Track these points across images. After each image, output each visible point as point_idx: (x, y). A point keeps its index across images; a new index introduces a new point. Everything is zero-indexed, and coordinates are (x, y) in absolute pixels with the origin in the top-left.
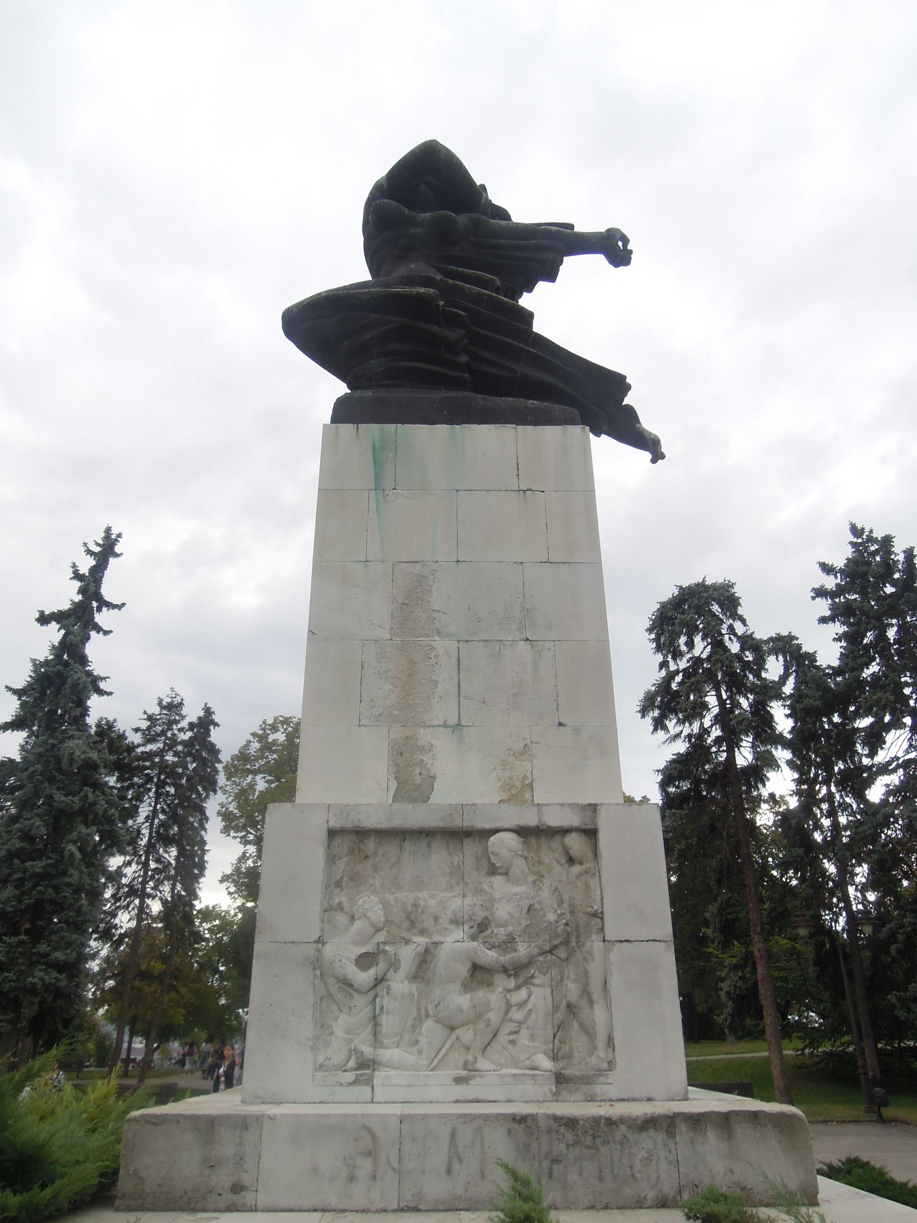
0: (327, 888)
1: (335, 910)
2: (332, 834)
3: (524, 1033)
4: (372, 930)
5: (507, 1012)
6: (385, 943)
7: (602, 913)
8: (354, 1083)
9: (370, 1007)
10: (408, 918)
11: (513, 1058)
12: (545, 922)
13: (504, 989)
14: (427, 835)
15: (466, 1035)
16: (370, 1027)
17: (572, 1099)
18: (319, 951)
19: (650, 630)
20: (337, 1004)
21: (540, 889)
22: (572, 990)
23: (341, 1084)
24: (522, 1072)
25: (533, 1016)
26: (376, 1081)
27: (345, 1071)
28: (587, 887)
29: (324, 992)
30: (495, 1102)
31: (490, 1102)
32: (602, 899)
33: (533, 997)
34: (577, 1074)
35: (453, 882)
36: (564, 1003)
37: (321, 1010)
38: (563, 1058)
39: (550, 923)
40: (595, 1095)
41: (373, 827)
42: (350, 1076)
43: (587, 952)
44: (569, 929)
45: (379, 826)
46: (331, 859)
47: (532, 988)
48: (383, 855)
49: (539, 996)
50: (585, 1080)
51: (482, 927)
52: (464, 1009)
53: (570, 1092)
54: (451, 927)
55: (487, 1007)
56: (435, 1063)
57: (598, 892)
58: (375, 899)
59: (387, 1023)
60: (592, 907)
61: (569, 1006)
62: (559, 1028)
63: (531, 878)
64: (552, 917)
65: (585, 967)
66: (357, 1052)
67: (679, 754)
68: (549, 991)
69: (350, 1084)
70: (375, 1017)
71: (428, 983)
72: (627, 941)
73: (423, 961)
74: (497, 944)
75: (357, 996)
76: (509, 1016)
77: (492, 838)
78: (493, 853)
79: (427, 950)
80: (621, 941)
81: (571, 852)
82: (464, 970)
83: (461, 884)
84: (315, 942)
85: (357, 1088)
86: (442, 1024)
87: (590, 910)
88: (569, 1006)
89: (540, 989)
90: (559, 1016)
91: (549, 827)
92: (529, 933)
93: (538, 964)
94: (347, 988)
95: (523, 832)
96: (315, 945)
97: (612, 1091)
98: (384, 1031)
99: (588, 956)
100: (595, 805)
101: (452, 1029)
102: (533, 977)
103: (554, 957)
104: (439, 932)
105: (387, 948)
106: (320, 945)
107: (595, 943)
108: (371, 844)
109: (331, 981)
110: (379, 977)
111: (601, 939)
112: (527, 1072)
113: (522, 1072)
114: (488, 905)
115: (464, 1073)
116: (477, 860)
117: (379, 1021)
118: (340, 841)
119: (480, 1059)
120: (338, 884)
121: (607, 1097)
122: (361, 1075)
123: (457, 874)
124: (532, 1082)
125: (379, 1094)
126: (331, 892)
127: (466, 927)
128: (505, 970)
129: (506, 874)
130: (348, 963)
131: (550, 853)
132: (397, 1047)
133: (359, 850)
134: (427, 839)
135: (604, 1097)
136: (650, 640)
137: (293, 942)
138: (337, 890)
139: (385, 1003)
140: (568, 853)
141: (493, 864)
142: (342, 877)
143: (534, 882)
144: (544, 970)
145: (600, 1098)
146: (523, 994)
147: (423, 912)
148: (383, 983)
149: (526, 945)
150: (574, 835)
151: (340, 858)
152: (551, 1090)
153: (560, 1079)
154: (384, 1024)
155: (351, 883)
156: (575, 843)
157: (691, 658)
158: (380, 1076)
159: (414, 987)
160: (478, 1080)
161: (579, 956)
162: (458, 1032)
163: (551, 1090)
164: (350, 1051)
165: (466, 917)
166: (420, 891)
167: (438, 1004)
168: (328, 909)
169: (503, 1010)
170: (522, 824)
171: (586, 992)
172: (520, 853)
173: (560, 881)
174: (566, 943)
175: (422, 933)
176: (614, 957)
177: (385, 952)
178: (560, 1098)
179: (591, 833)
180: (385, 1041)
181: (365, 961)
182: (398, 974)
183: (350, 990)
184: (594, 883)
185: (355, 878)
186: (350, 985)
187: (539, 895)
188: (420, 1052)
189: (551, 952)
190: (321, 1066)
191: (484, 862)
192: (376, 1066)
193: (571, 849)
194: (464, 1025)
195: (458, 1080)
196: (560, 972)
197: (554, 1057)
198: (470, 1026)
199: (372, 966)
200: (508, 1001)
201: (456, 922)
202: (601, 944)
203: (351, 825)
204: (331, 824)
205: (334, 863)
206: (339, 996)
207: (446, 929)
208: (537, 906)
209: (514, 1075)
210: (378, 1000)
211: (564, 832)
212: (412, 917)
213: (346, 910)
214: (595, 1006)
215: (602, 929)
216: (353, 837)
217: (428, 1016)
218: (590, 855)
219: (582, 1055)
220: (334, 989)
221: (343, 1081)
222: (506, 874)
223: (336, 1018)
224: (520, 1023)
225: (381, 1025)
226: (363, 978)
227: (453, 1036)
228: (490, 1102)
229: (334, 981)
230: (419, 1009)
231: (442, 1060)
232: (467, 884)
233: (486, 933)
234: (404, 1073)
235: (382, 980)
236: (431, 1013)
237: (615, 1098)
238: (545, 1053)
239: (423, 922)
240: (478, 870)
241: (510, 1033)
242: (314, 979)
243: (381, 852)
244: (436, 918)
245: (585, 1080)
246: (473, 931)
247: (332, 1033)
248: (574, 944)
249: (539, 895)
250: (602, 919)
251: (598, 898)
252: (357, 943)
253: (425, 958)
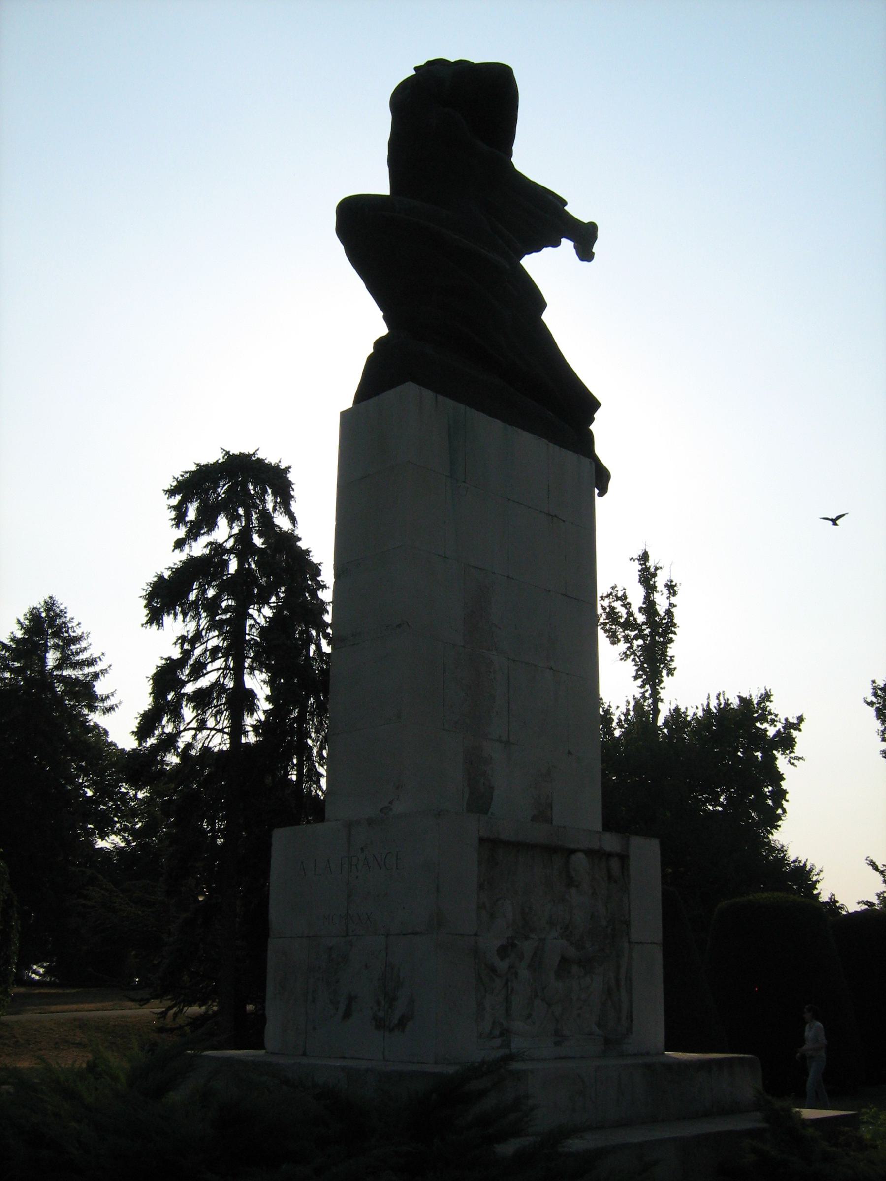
2: (482, 840)
19: (171, 492)
67: (169, 659)
95: (589, 853)
136: (170, 507)
156: (615, 864)
157: (210, 543)
177: (514, 945)
181: (503, 952)
210: (510, 984)
211: (609, 855)
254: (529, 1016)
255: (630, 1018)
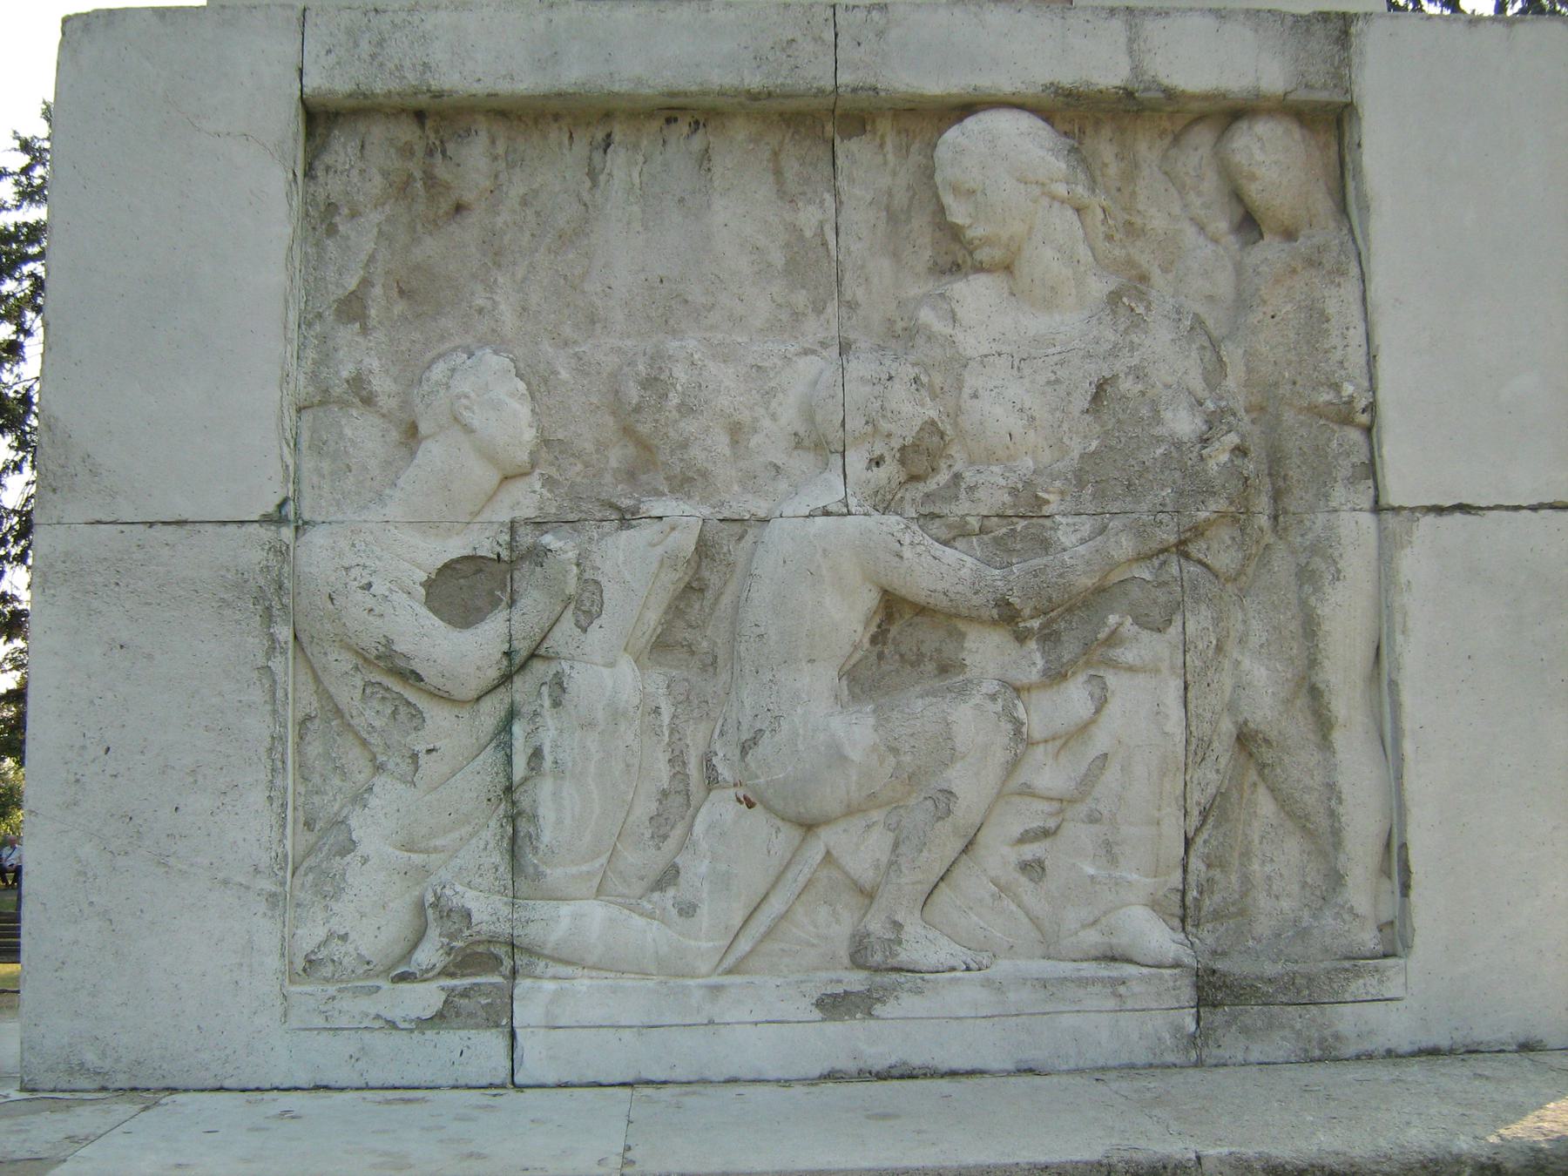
0: (305, 322)
1: (344, 404)
2: (319, 119)
3: (1078, 833)
4: (484, 475)
5: (1013, 765)
6: (539, 525)
7: (1372, 408)
8: (440, 1019)
9: (490, 756)
10: (627, 431)
11: (1035, 921)
12: (1159, 440)
13: (1005, 683)
14: (696, 126)
15: (861, 848)
16: (493, 823)
17: (1255, 1056)
18: (282, 552)
20: (364, 743)
21: (1137, 323)
22: (1261, 685)
23: (392, 1025)
24: (1066, 968)
25: (1112, 775)
26: (524, 1014)
27: (404, 977)
28: (1316, 318)
29: (309, 701)
30: (971, 1073)
31: (953, 1074)
32: (1371, 359)
33: (1114, 707)
34: (1270, 969)
35: (801, 299)
36: (1227, 726)
37: (301, 766)
38: (1217, 916)
39: (1178, 445)
40: (1337, 1037)
41: (479, 89)
42: (426, 997)
43: (1314, 549)
44: (1250, 467)
45: (504, 87)
46: (322, 219)
47: (1111, 679)
48: (524, 202)
49: (1138, 710)
50: (1302, 991)
51: (919, 457)
52: (855, 755)
53: (1245, 1030)
54: (801, 463)
55: (945, 750)
56: (744, 945)
57: (1357, 335)
58: (494, 362)
59: (557, 810)
60: (1336, 387)
61: (1245, 740)
62: (1205, 814)
63: (1099, 287)
64: (1183, 423)
65: (1303, 603)
66: (446, 912)
68: (1174, 686)
69: (423, 1024)
70: (509, 790)
71: (710, 665)
72: (1463, 508)
73: (689, 587)
74: (974, 523)
75: (438, 717)
76: (1023, 776)
77: (952, 134)
78: (955, 189)
79: (704, 549)
80: (1439, 510)
81: (1253, 191)
82: (847, 616)
83: (832, 308)
84: (266, 520)
85: (451, 1039)
86: (769, 808)
87: (1325, 396)
88: (1245, 740)
89: (1141, 679)
90: (1209, 777)
91: (1170, 95)
92: (1097, 480)
93: (1135, 592)
94: (396, 686)
95: (1071, 112)
96: (266, 533)
97: (1396, 1025)
98: (546, 837)
99: (1318, 563)
100: (1346, 19)
101: (809, 826)
102: (1113, 640)
103: (1194, 569)
104: (749, 481)
105: (548, 539)
106: (287, 533)
107: (1344, 516)
108: (474, 161)
109: (338, 662)
110: (523, 647)
111: (1367, 503)
112: (1089, 969)
113: (1066, 968)
114: (938, 379)
115: (856, 981)
116: (892, 218)
117: (525, 803)
118: (352, 148)
119: (913, 928)
120: (352, 308)
121: (1378, 1043)
122: (465, 993)
123: (812, 269)
124: (1111, 1003)
125: (536, 1060)
126: (324, 339)
127: (857, 461)
128: (1007, 615)
129: (1008, 268)
130: (400, 598)
131: (1174, 200)
132: (599, 892)
133: (430, 180)
134: (697, 143)
135: (1367, 1046)
137: (181, 523)
138: (347, 334)
139: (547, 739)
140: (1237, 196)
141: (955, 233)
142: (366, 283)
143: (1114, 298)
144: (1156, 614)
145: (1351, 1050)
146: (1075, 698)
147: (686, 409)
148: (538, 667)
149: (1087, 526)
150: (1263, 128)
151: (354, 214)
152: (1177, 1029)
153: (1212, 990)
154: (547, 813)
155: (400, 307)
156: (1271, 158)
158: (534, 1000)
159: (656, 681)
160: (907, 1004)
161: (1282, 565)
162: (827, 837)
163: (1177, 1029)
164: (420, 907)
165: (855, 423)
166: (674, 333)
167: (754, 741)
168: (321, 401)
169: (1000, 756)
170: (1067, 77)
171: (1312, 695)
172: (1061, 189)
173: (1210, 298)
174: (1239, 518)
175: (683, 484)
176: (1413, 564)
177: (538, 555)
178: (1211, 1053)
179: (1329, 122)
180: (555, 874)
181: (464, 588)
182: (595, 634)
183: (410, 695)
184: (1340, 301)
185: (419, 293)
186: (412, 677)
187: (1133, 348)
188: (688, 910)
189: (1181, 549)
190: (311, 963)
191: (920, 224)
192: (521, 960)
193: (1253, 177)
194: (850, 811)
195: (833, 1005)
196: (1217, 621)
197: (1185, 916)
198: (876, 815)
199: (495, 603)
200: (1018, 724)
201: (821, 445)
202: (1367, 520)
203: (394, 86)
204: (315, 81)
205: (332, 230)
206: (371, 716)
207: (777, 468)
208: (1127, 385)
209: (1044, 983)
210: (518, 729)
211: (1231, 113)
212: (644, 429)
213: (386, 403)
214: (1337, 736)
215: (1371, 469)
216: (407, 132)
217: (712, 780)
218: (1323, 204)
219: (1285, 904)
220: (348, 694)
221: (396, 1014)
222: (1008, 268)
223: (360, 798)
224: (1064, 802)
225: (534, 818)
226: (466, 651)
227: (815, 852)
228: (953, 1074)
229: (346, 661)
230: (677, 760)
231: (768, 934)
232: (852, 306)
233: (931, 485)
234: (628, 982)
235: (533, 655)
236: (724, 772)
237: (1406, 1047)
238: (1155, 905)
239: (684, 445)
240: (896, 255)
241: (1022, 840)
242: (271, 651)
243: (516, 189)
244: (736, 432)
245: (1302, 991)
246: (881, 474)
247: (349, 847)
248: (1263, 521)
249: (1133, 348)
250: (1368, 430)
251: (1357, 358)
252: (425, 525)
253: (699, 580)
254: (669, 876)
255: (1395, 862)
